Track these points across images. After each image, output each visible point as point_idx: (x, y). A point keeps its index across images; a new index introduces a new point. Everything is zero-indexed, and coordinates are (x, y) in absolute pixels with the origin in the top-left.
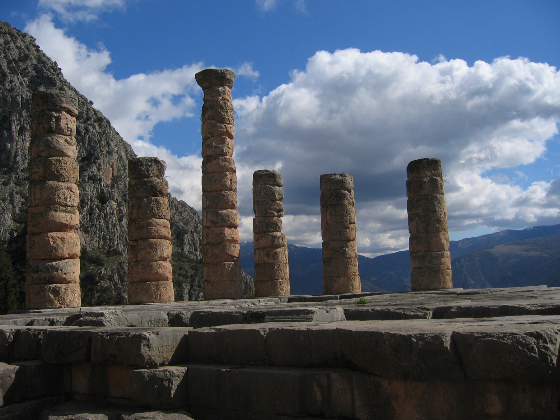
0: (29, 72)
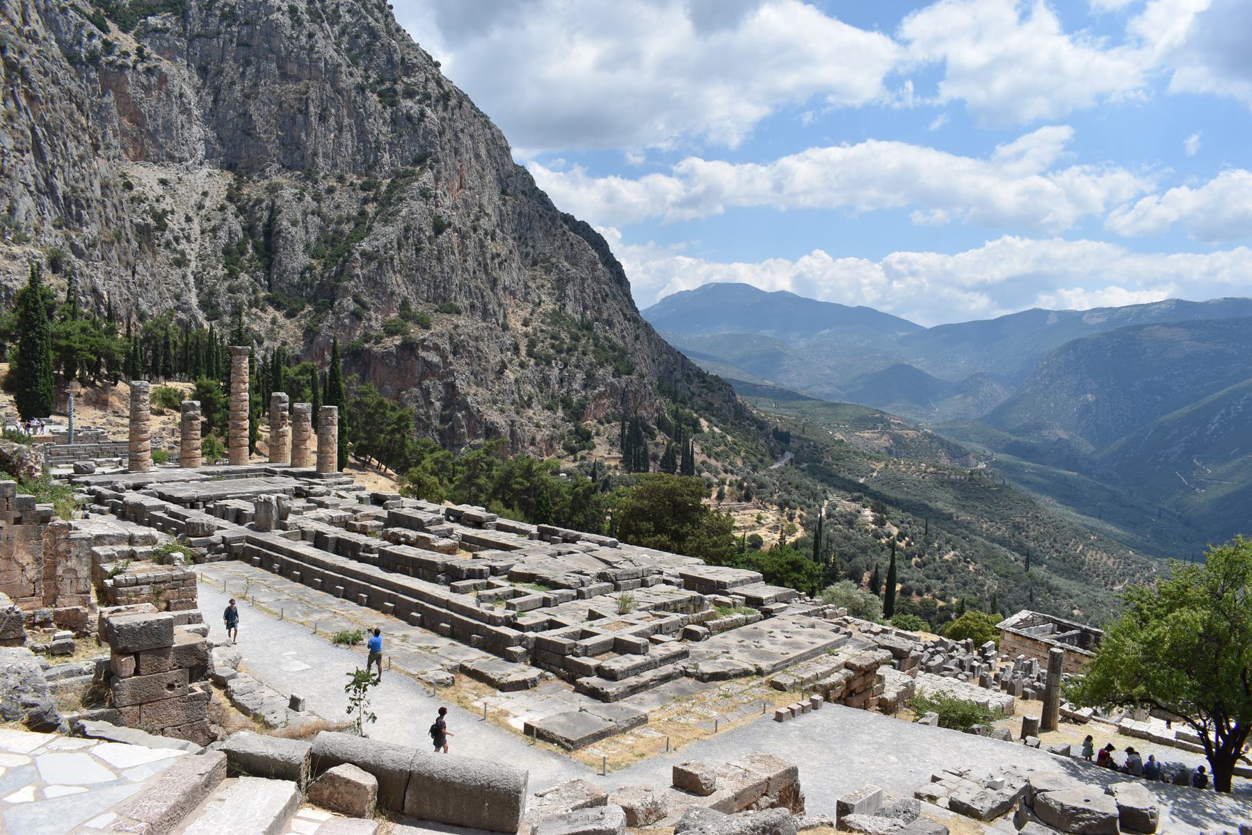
0: (340, 17)
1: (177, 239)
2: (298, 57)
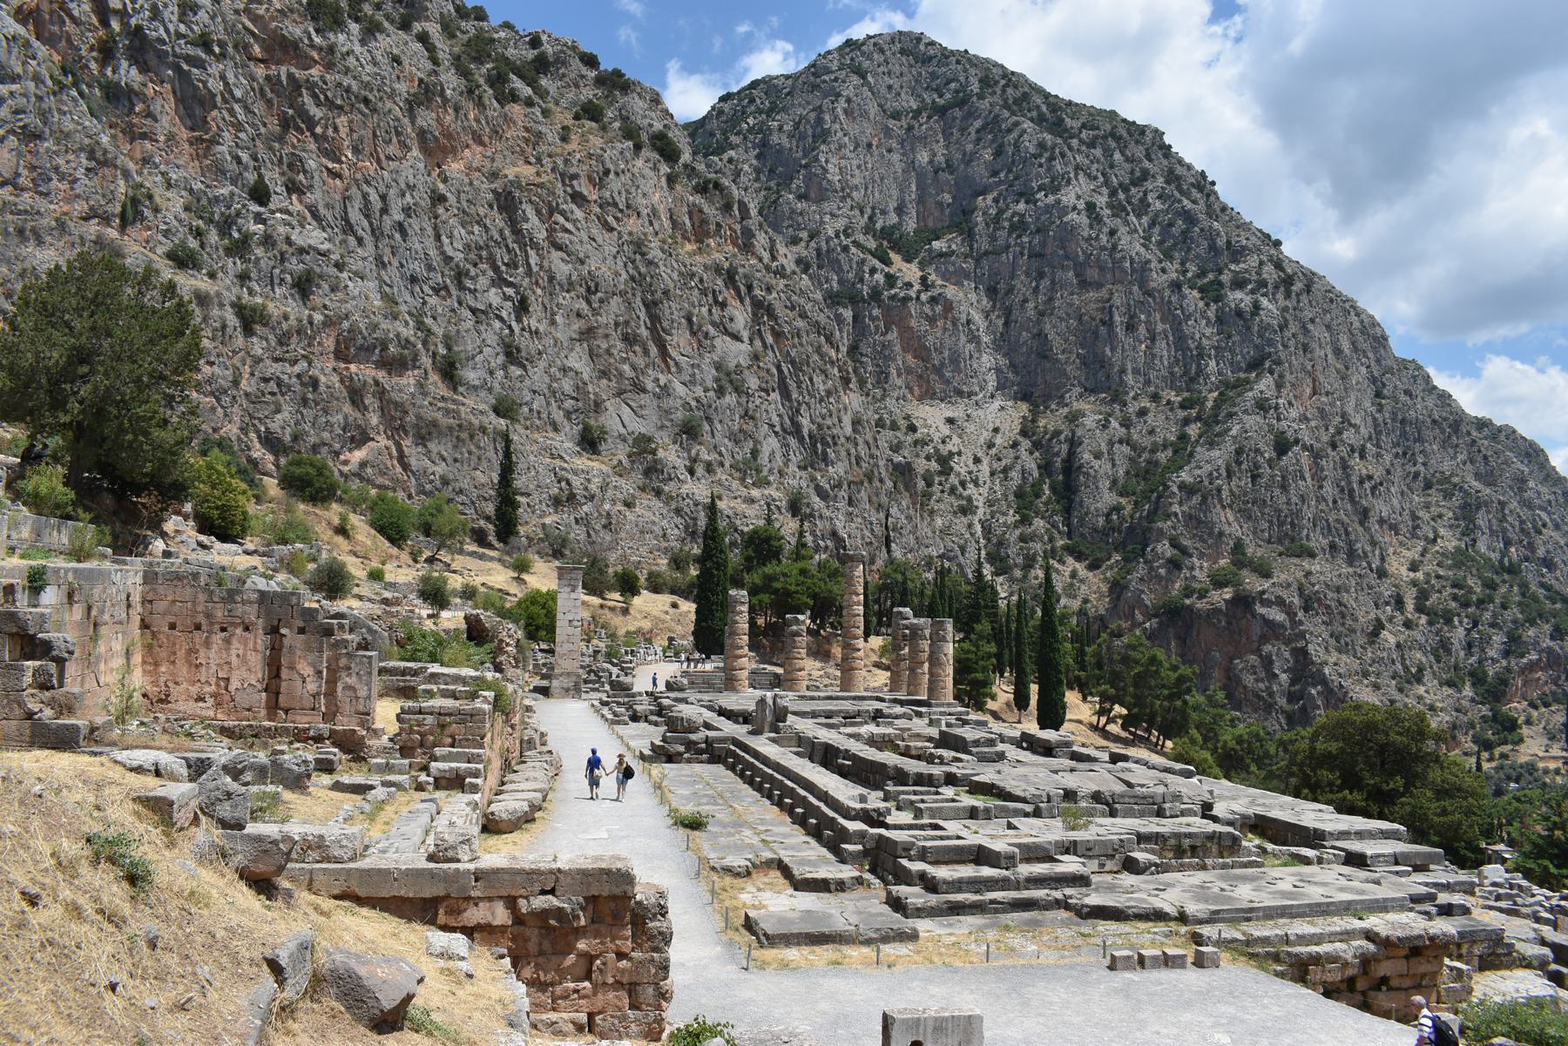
0: (1149, 205)
1: (963, 484)
2: (1098, 259)
